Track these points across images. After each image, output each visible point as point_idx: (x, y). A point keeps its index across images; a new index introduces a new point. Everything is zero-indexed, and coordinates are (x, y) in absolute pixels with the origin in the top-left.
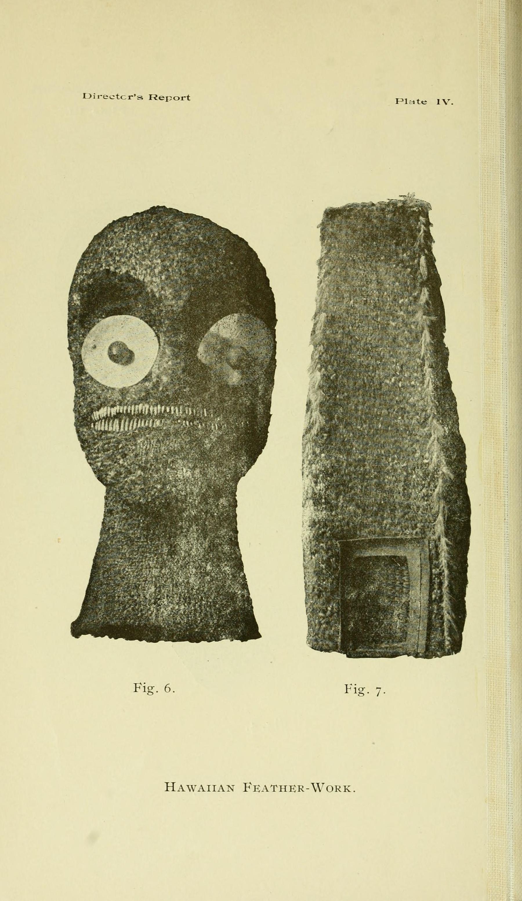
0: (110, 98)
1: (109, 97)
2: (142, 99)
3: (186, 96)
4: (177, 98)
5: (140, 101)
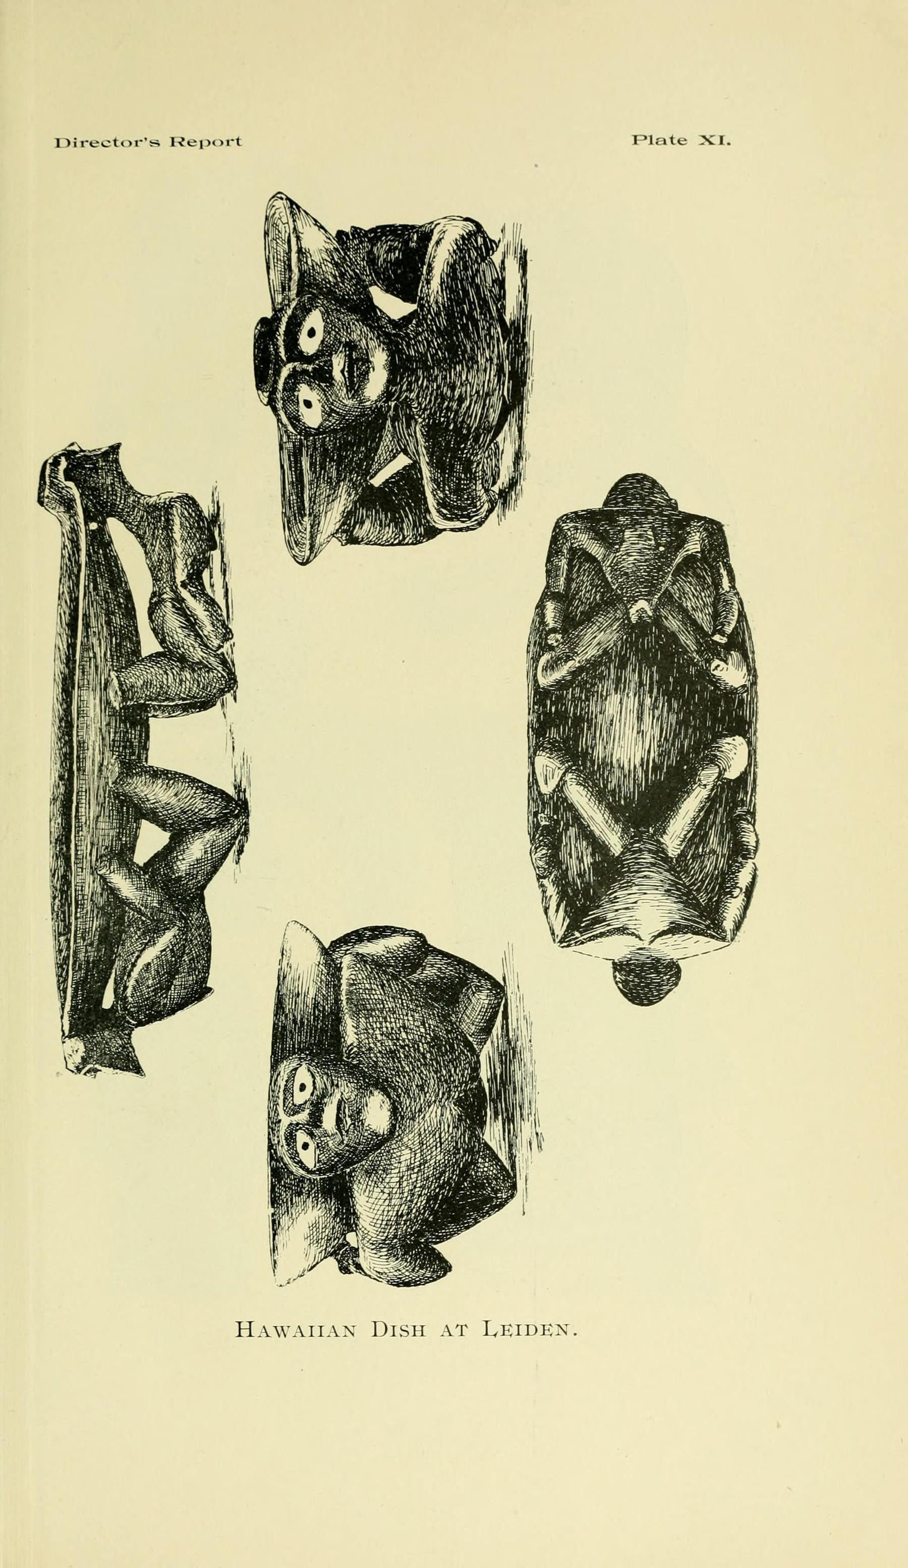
0: (103, 145)
2: (159, 144)
4: (218, 143)
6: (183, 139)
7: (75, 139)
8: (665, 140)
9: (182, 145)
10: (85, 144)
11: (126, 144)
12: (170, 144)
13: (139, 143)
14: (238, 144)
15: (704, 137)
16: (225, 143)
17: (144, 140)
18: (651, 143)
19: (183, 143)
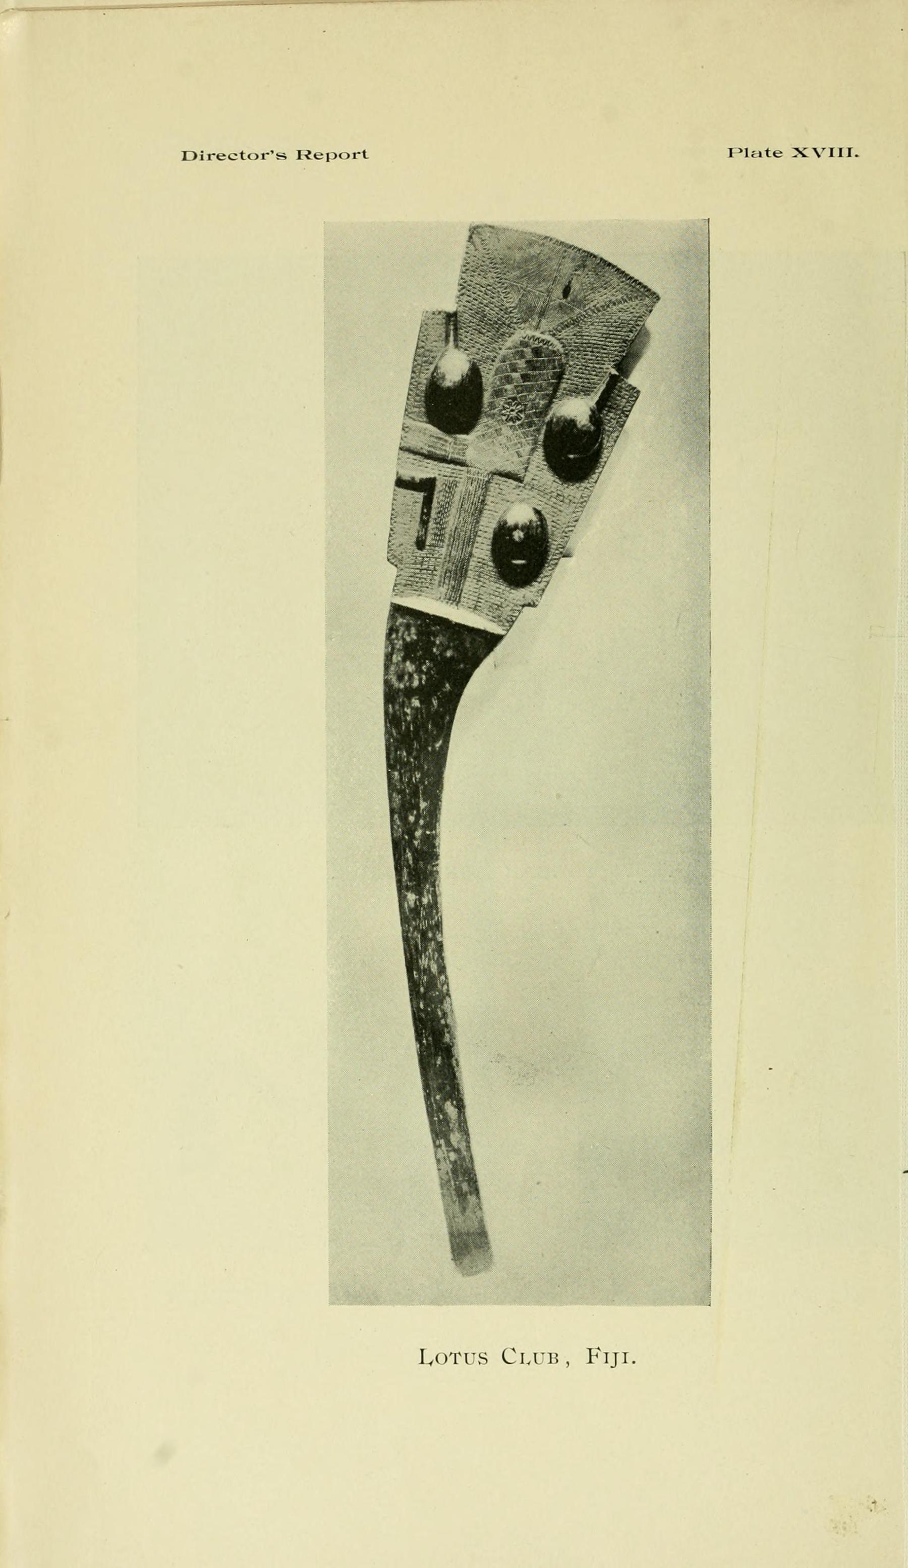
0: (229, 158)
1: (227, 156)
2: (285, 157)
3: (361, 151)
4: (344, 156)
5: (282, 161)
6: (309, 152)
7: (202, 152)
8: (760, 153)
9: (308, 158)
10: (212, 157)
11: (253, 157)
12: (297, 156)
14: (364, 156)
15: (797, 149)
17: (271, 153)
18: (747, 156)
19: (309, 156)
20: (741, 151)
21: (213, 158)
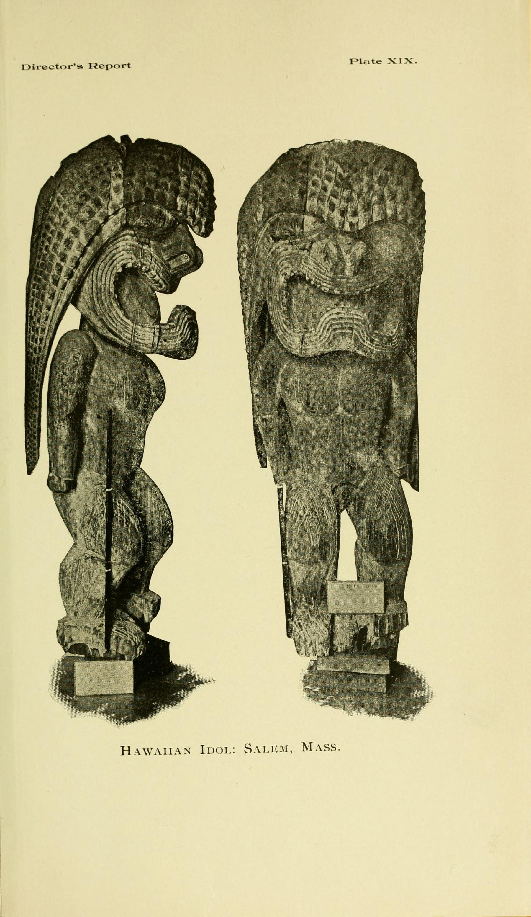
0: (50, 68)
2: (82, 68)
3: (127, 63)
5: (80, 70)
10: (39, 68)
11: (63, 67)
13: (71, 67)
15: (390, 59)
16: (121, 66)
18: (361, 63)
20: (357, 60)
21: (40, 68)
